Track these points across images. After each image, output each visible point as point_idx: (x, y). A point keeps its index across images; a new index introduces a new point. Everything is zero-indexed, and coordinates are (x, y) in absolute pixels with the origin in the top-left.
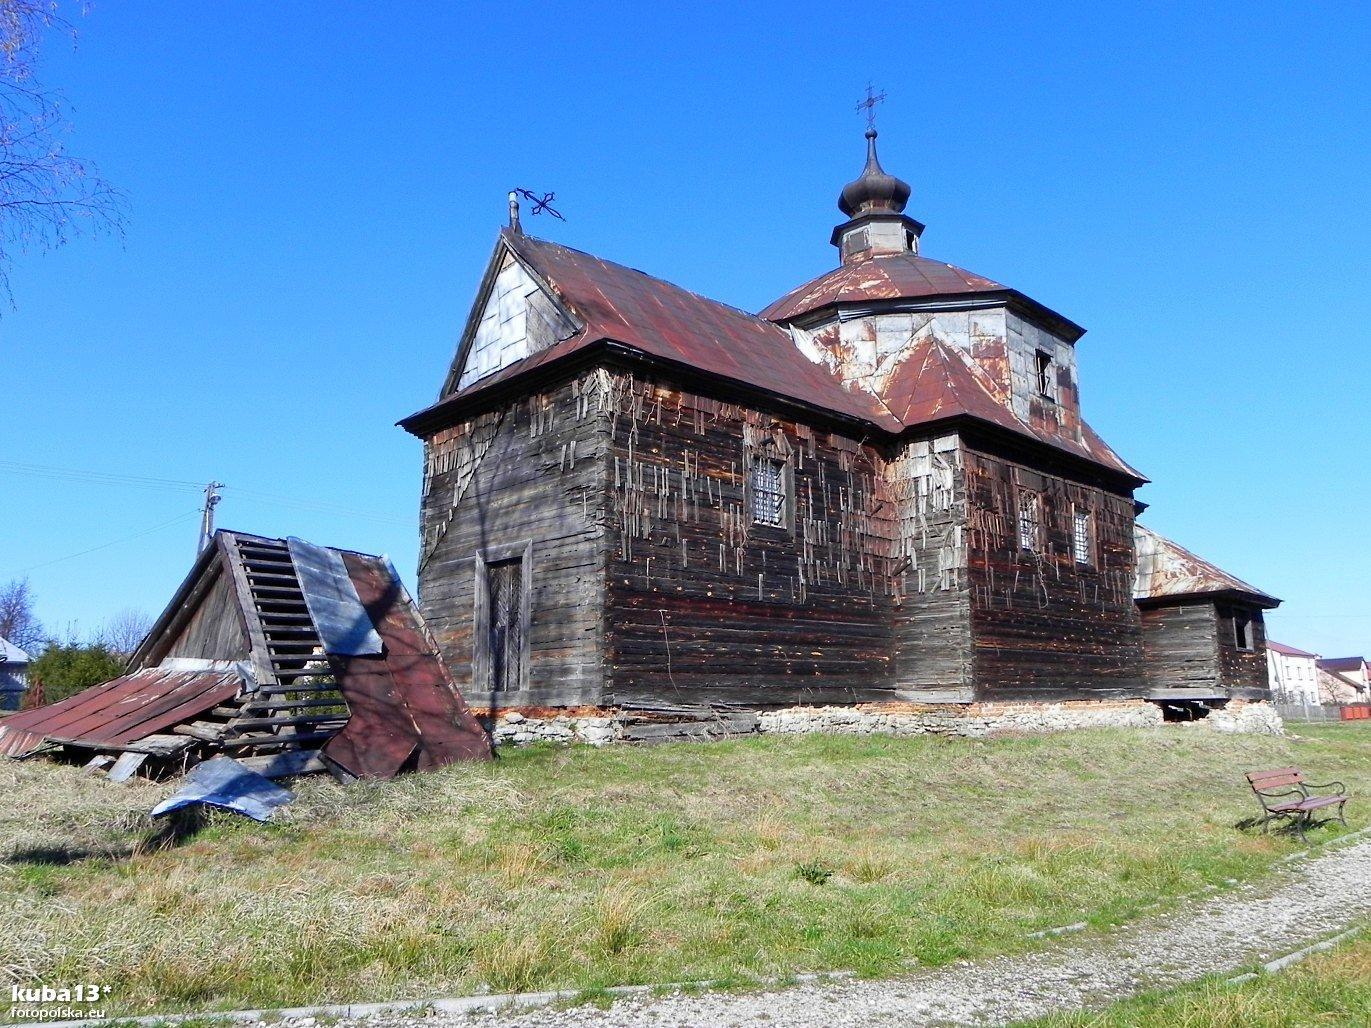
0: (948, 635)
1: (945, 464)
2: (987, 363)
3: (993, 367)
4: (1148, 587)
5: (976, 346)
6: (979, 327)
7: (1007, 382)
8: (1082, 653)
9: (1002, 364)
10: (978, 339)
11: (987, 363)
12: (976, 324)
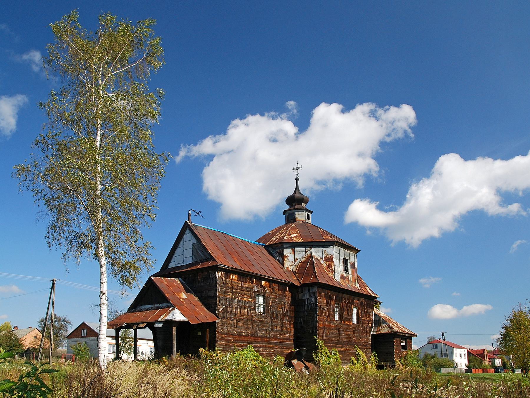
2: (328, 263)
4: (376, 330)
5: (325, 258)
6: (326, 251)
7: (333, 269)
9: (333, 263)
10: (326, 255)
11: (328, 263)
12: (325, 251)
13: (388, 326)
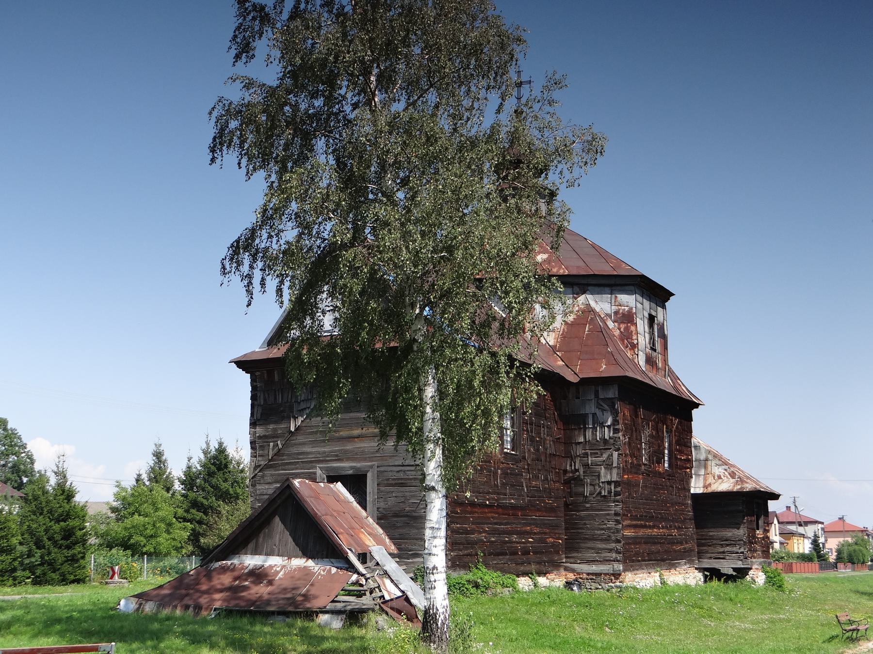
0: (605, 526)
1: (606, 407)
2: (623, 326)
3: (627, 329)
4: (701, 485)
7: (635, 342)
8: (668, 535)
10: (617, 308)
11: (623, 326)
13: (731, 476)
